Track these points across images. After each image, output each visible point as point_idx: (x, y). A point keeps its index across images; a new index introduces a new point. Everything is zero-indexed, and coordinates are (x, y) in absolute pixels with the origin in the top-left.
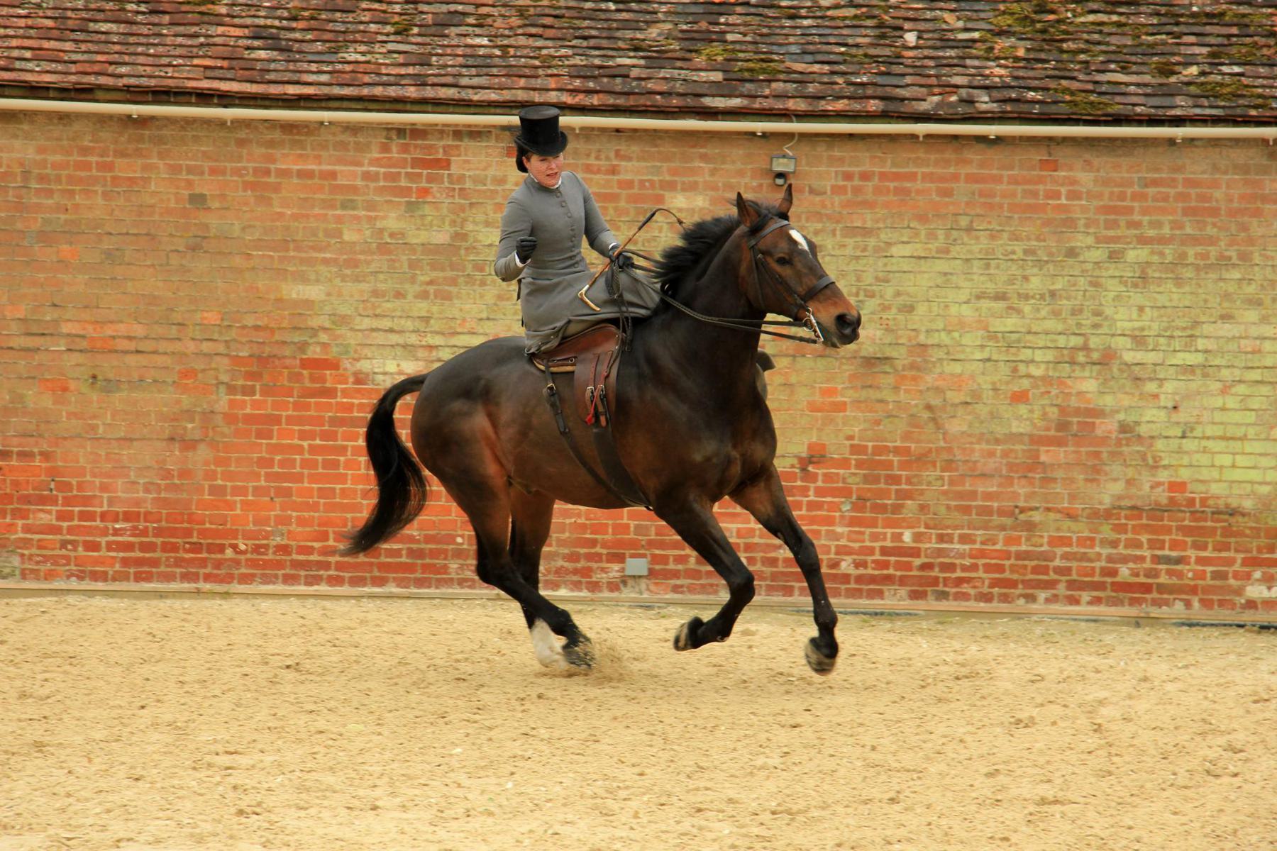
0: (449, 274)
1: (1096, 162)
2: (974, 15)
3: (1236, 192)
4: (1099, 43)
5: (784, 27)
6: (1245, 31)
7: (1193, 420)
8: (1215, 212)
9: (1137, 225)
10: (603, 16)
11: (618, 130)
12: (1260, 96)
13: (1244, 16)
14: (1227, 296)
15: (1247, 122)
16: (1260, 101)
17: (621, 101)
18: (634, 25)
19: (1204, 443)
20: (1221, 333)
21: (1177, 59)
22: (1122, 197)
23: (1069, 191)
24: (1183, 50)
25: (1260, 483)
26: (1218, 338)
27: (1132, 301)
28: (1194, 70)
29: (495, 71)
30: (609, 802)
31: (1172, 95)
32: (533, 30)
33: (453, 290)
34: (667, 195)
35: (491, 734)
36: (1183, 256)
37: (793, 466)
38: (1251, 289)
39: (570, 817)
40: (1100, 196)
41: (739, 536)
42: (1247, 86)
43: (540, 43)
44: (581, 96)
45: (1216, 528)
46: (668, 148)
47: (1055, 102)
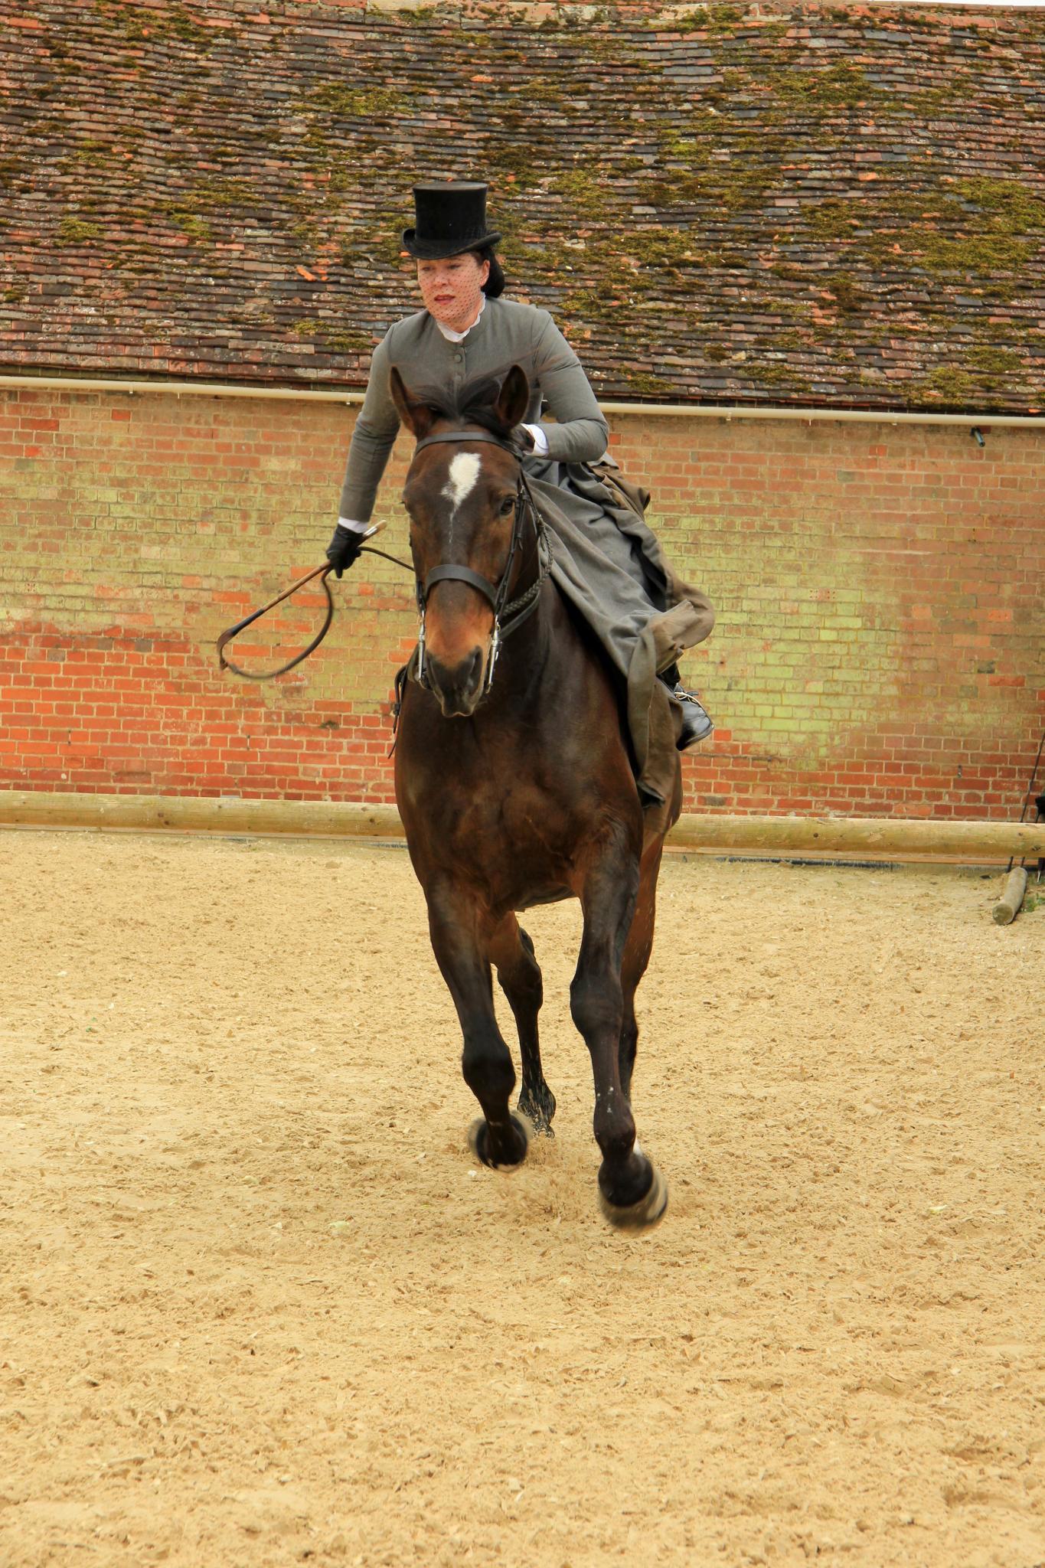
0: (56, 527)
1: (654, 437)
2: (546, 300)
3: (778, 468)
4: (658, 328)
5: (371, 305)
6: (788, 321)
7: (738, 674)
8: (760, 485)
9: (689, 495)
10: (203, 290)
11: (216, 397)
12: (800, 381)
13: (787, 307)
14: (769, 562)
15: (789, 404)
16: (801, 385)
17: (220, 370)
18: (232, 299)
19: (747, 695)
20: (764, 596)
21: (728, 344)
22: (677, 469)
23: (630, 464)
24: (733, 336)
25: (796, 733)
26: (760, 600)
27: (685, 565)
28: (742, 355)
29: (101, 339)
30: (205, 1022)
31: (724, 378)
32: (138, 302)
33: (62, 543)
34: (262, 458)
35: (93, 958)
36: (731, 524)
37: (375, 712)
38: (790, 556)
39: (168, 1036)
40: (658, 468)
41: (325, 775)
42: (789, 371)
43: (144, 314)
44: (183, 364)
45: (756, 773)
46: (262, 414)
47: (618, 382)
